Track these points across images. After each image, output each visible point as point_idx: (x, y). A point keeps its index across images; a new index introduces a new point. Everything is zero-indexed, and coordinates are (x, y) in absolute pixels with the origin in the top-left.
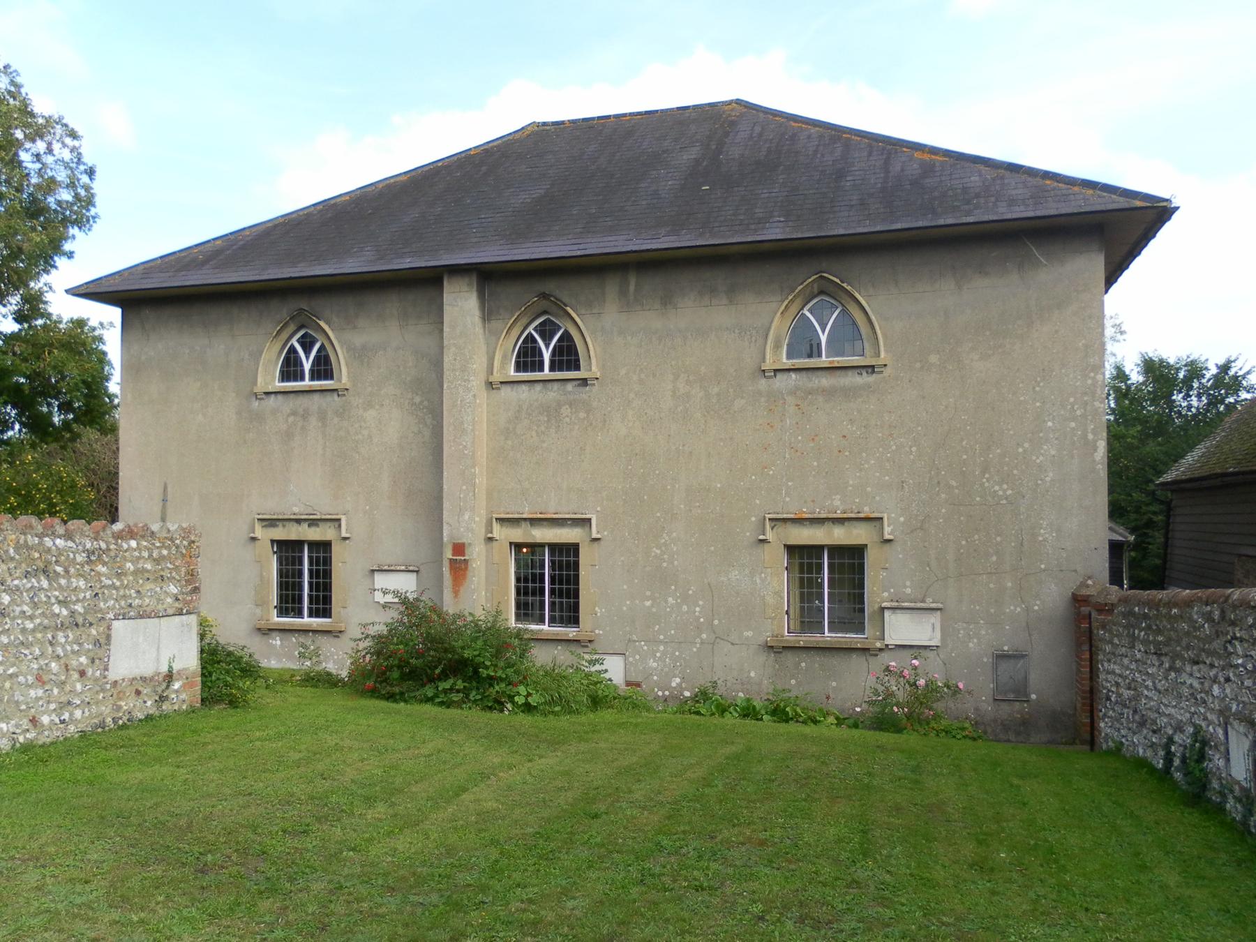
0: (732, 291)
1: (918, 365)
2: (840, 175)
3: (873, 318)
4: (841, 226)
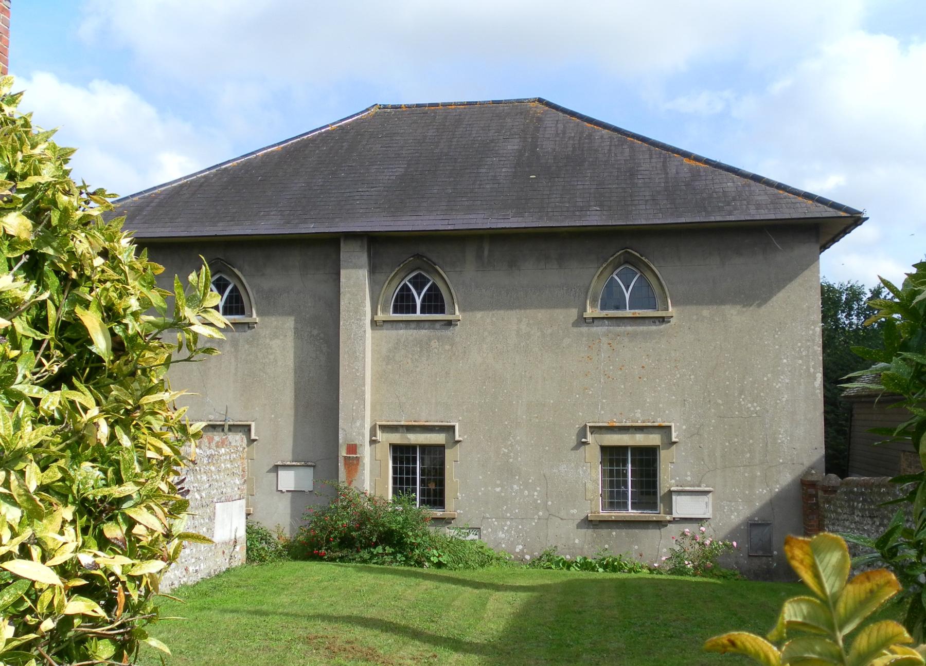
1: (695, 317)
2: (632, 173)
3: (663, 282)
4: (644, 217)
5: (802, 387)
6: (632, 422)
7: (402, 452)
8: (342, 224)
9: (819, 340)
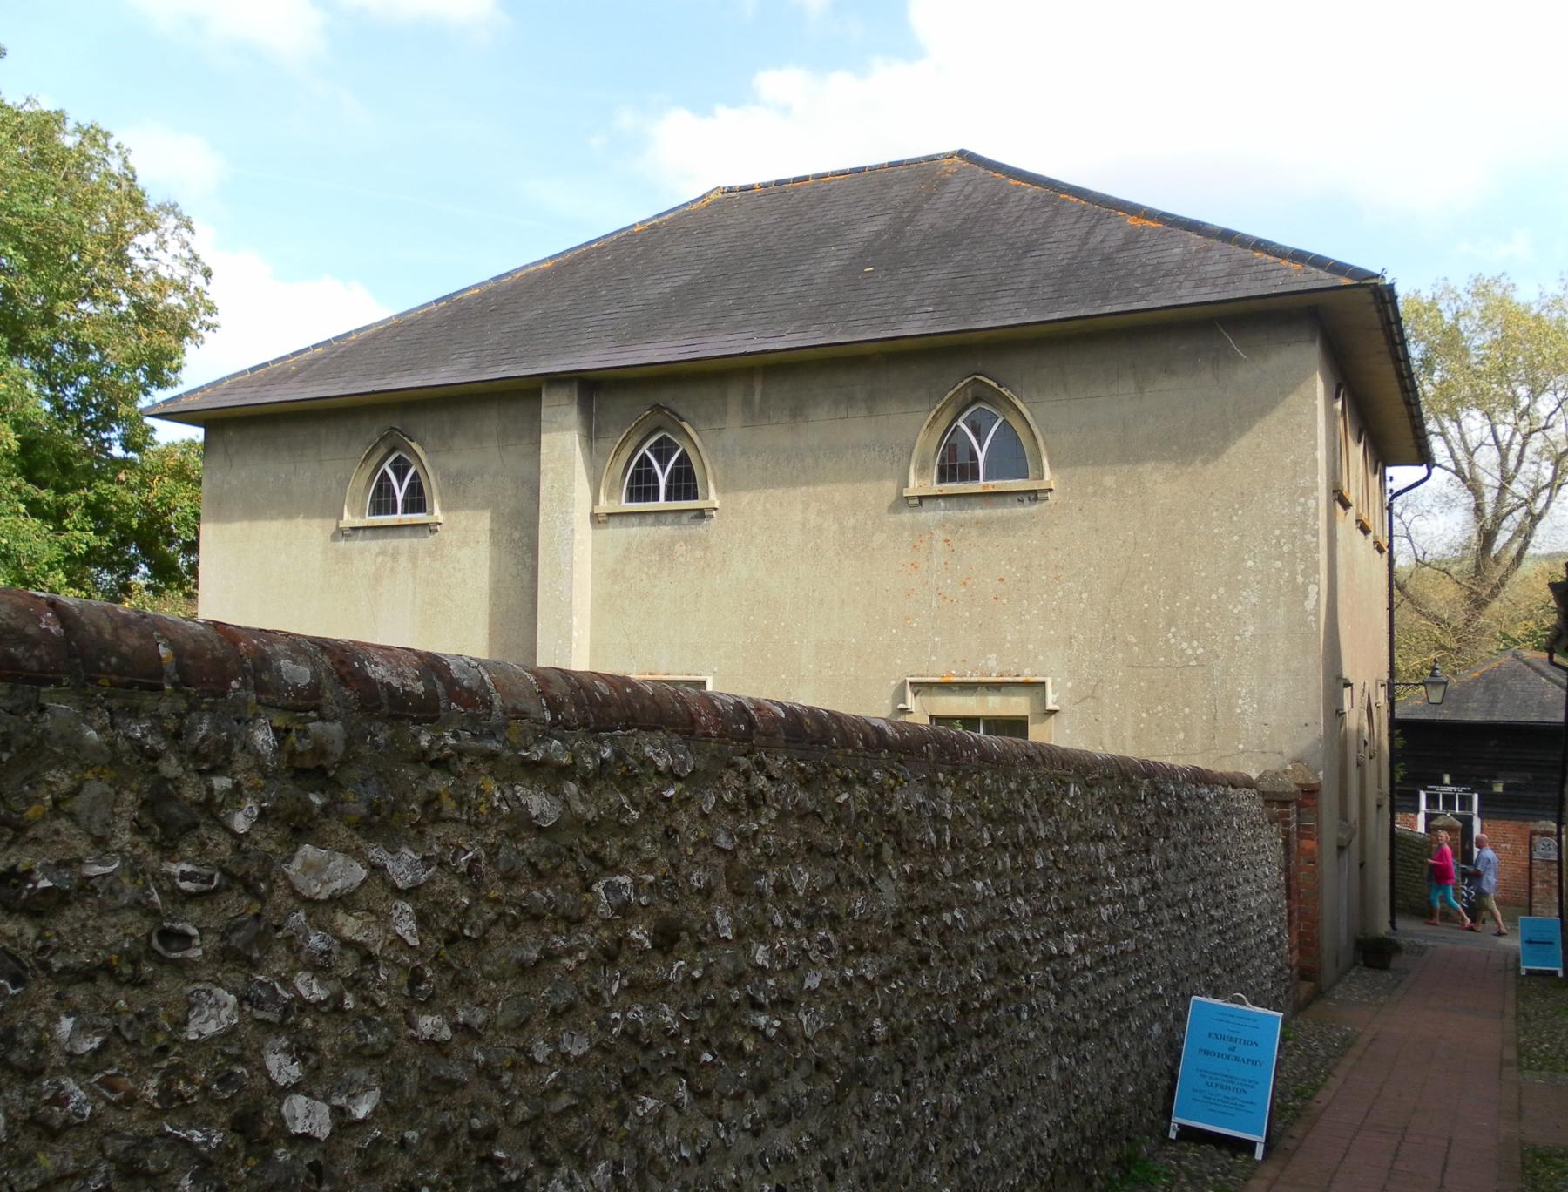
0: (872, 400)
1: (1090, 489)
3: (1036, 430)
5: (1282, 611)
6: (983, 675)
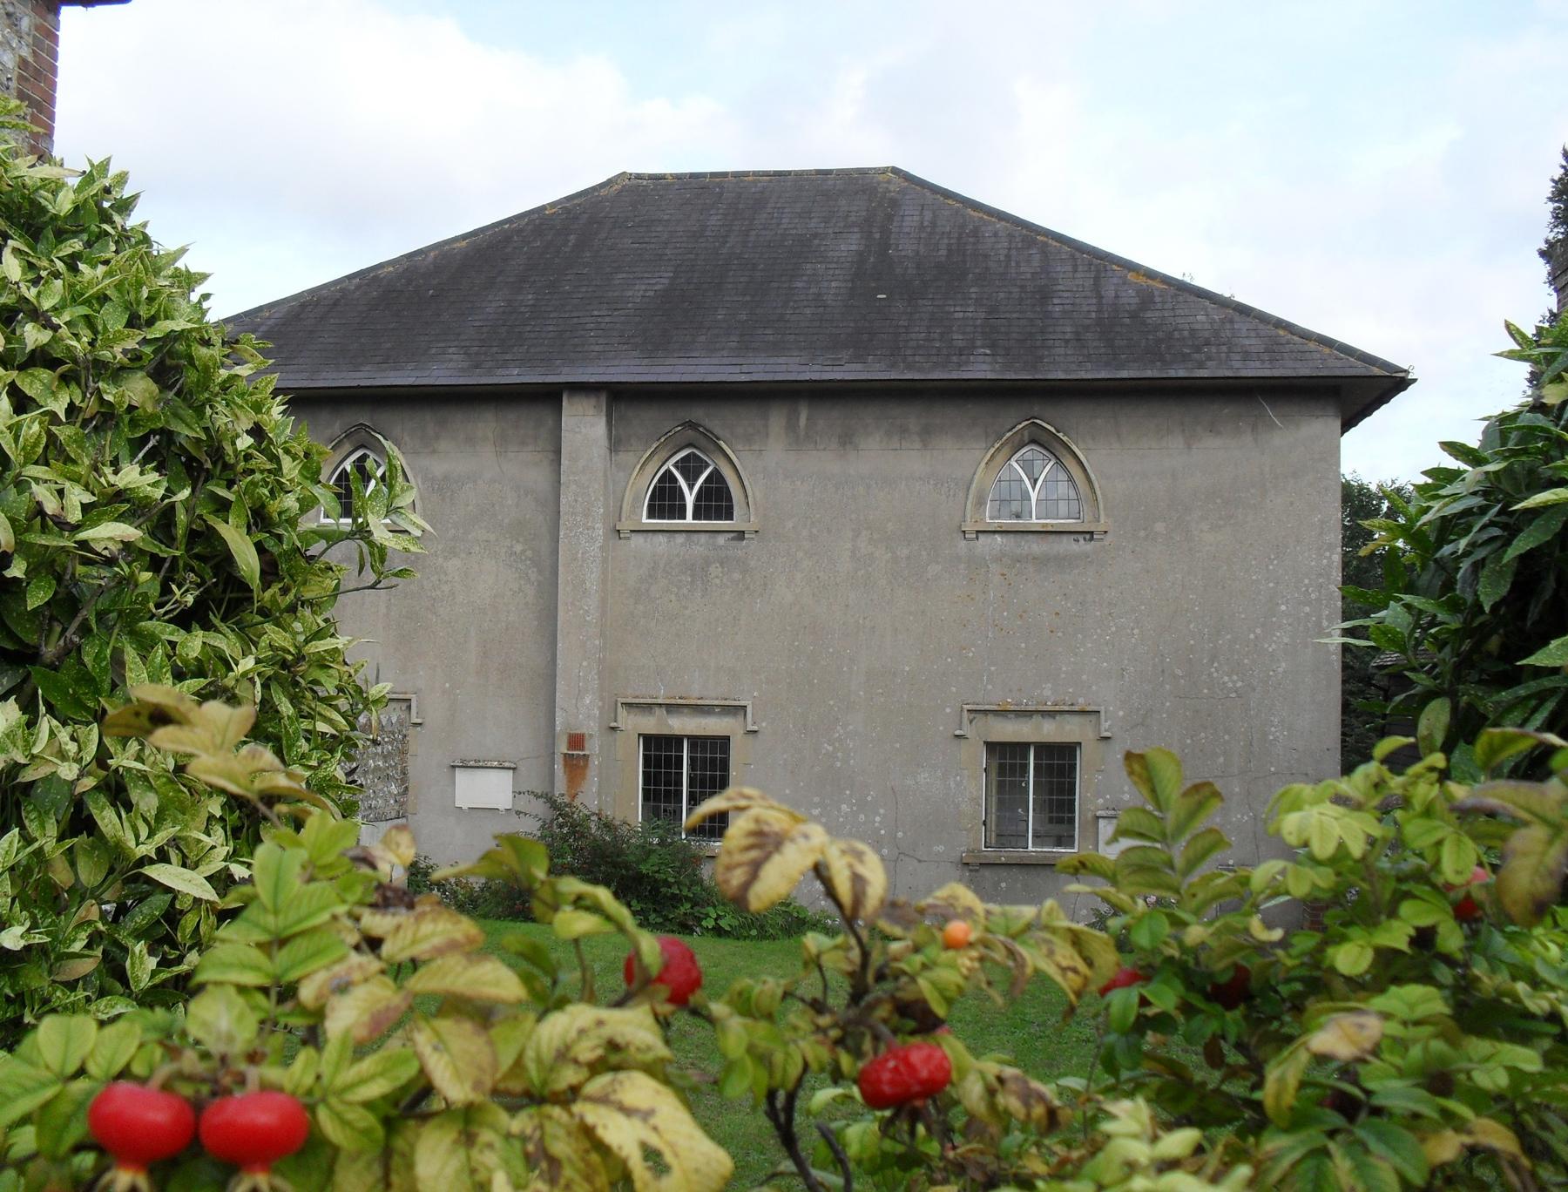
0: (926, 433)
1: (1142, 533)
2: (1044, 295)
7: (658, 749)
8: (565, 370)
9: (1337, 576)
